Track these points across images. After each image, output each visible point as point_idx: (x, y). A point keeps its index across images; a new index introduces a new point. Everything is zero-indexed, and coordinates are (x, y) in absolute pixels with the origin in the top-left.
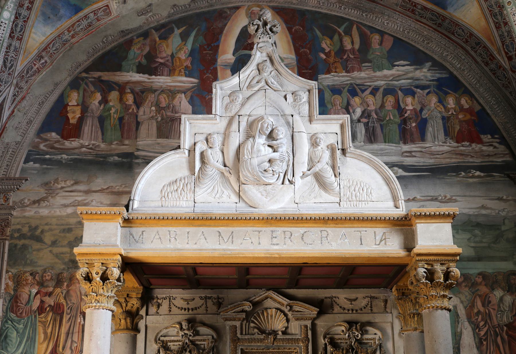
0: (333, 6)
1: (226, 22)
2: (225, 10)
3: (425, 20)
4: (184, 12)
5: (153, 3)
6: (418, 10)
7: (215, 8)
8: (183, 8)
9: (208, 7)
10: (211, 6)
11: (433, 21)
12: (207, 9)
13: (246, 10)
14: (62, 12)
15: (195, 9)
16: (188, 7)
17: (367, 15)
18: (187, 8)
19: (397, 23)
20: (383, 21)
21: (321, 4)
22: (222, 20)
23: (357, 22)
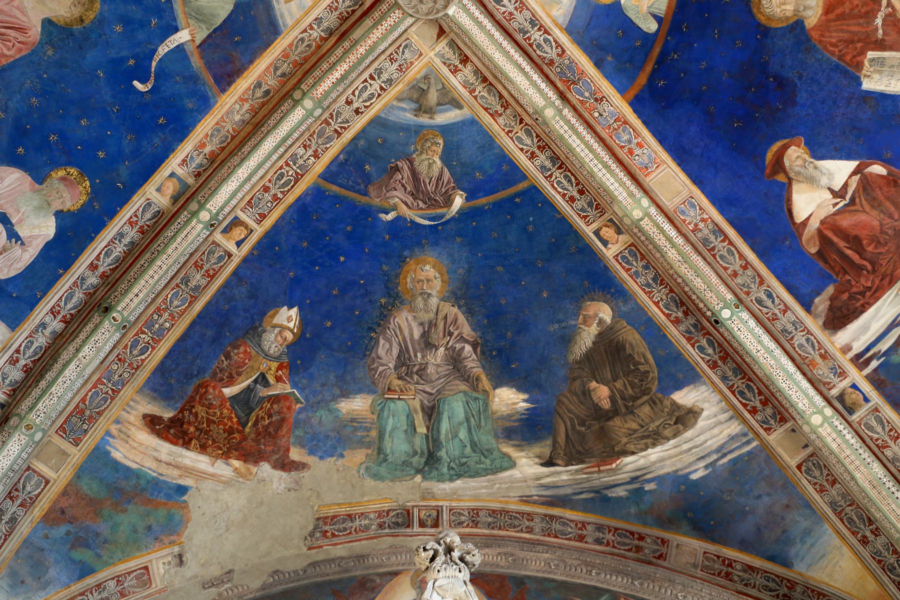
0: (576, 570)
1: (374, 595)
2: (372, 577)
3: (754, 590)
4: (292, 582)
5: (236, 568)
6: (737, 572)
7: (352, 574)
8: (292, 575)
9: (339, 573)
10: (346, 571)
11: (771, 590)
12: (337, 577)
13: (412, 576)
14: (52, 573)
15: (315, 577)
16: (301, 573)
17: (641, 584)
18: (299, 574)
19: (701, 596)
20: (674, 592)
21: (553, 567)
22: (366, 593)
23: (625, 594)
